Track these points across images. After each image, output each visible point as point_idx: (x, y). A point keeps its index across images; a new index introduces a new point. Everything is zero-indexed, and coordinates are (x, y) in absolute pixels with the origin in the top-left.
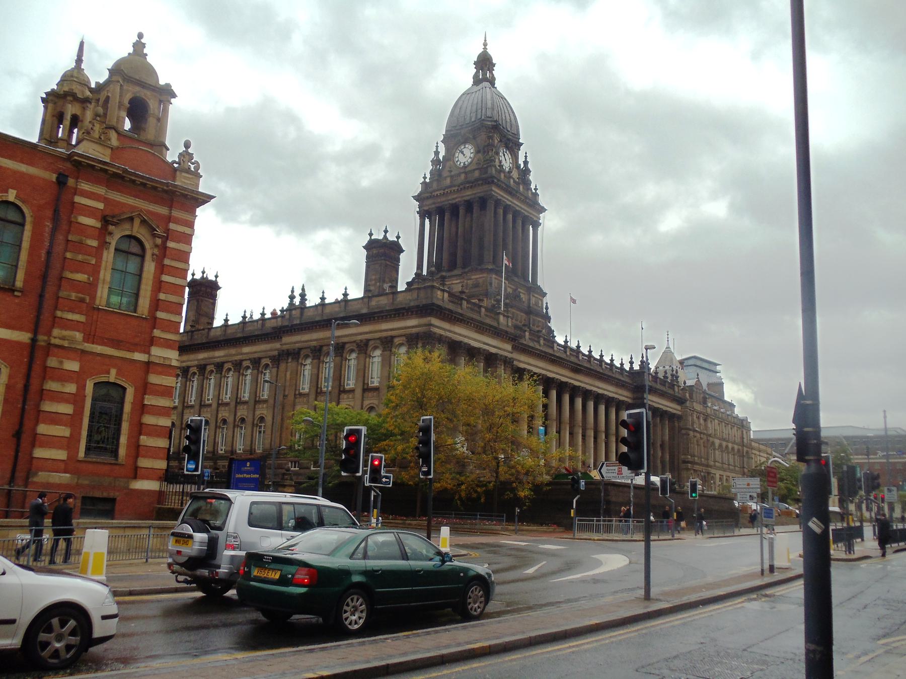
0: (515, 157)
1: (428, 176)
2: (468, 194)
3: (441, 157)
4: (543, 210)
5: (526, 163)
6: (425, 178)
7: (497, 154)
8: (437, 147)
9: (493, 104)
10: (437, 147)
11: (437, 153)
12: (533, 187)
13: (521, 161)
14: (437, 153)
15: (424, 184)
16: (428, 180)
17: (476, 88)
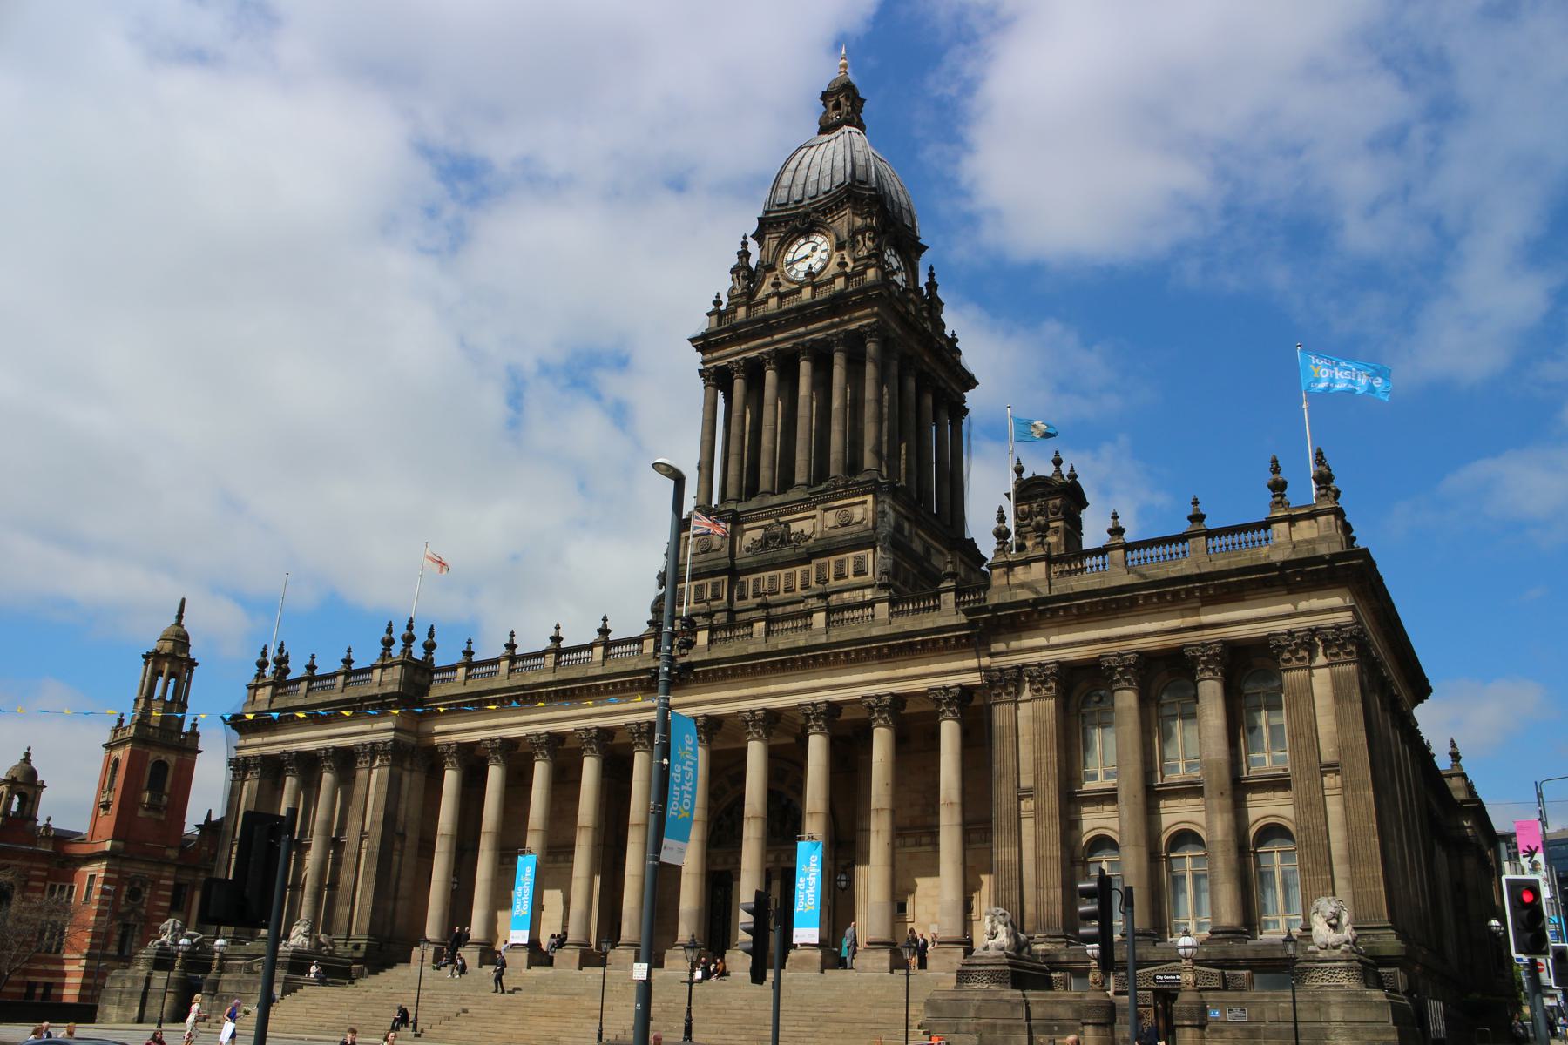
0: (913, 273)
1: (725, 300)
2: (816, 331)
3: (753, 263)
4: (970, 382)
5: (932, 285)
6: (717, 303)
7: (883, 253)
8: (745, 244)
9: (867, 161)
10: (745, 244)
11: (744, 254)
12: (948, 333)
13: (923, 280)
14: (744, 254)
15: (717, 313)
16: (723, 308)
17: (825, 137)
